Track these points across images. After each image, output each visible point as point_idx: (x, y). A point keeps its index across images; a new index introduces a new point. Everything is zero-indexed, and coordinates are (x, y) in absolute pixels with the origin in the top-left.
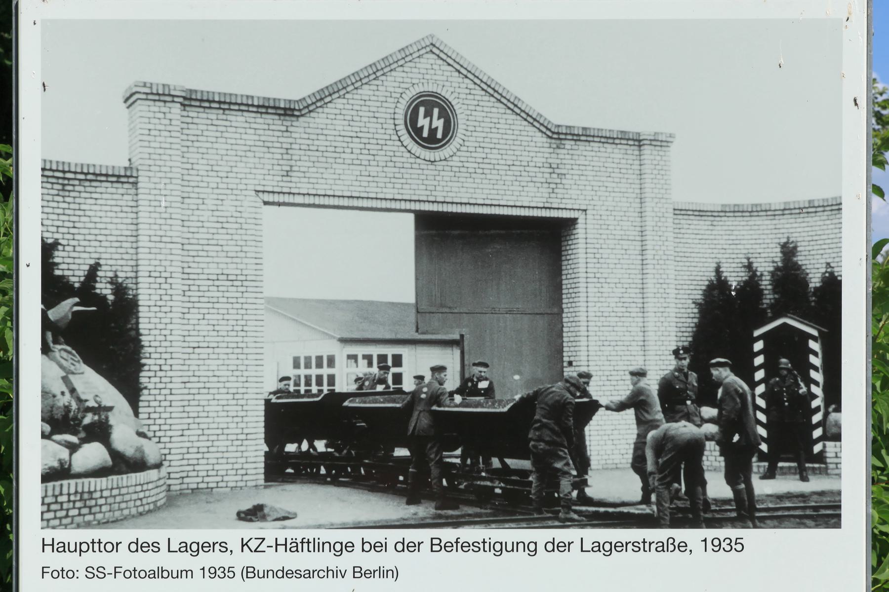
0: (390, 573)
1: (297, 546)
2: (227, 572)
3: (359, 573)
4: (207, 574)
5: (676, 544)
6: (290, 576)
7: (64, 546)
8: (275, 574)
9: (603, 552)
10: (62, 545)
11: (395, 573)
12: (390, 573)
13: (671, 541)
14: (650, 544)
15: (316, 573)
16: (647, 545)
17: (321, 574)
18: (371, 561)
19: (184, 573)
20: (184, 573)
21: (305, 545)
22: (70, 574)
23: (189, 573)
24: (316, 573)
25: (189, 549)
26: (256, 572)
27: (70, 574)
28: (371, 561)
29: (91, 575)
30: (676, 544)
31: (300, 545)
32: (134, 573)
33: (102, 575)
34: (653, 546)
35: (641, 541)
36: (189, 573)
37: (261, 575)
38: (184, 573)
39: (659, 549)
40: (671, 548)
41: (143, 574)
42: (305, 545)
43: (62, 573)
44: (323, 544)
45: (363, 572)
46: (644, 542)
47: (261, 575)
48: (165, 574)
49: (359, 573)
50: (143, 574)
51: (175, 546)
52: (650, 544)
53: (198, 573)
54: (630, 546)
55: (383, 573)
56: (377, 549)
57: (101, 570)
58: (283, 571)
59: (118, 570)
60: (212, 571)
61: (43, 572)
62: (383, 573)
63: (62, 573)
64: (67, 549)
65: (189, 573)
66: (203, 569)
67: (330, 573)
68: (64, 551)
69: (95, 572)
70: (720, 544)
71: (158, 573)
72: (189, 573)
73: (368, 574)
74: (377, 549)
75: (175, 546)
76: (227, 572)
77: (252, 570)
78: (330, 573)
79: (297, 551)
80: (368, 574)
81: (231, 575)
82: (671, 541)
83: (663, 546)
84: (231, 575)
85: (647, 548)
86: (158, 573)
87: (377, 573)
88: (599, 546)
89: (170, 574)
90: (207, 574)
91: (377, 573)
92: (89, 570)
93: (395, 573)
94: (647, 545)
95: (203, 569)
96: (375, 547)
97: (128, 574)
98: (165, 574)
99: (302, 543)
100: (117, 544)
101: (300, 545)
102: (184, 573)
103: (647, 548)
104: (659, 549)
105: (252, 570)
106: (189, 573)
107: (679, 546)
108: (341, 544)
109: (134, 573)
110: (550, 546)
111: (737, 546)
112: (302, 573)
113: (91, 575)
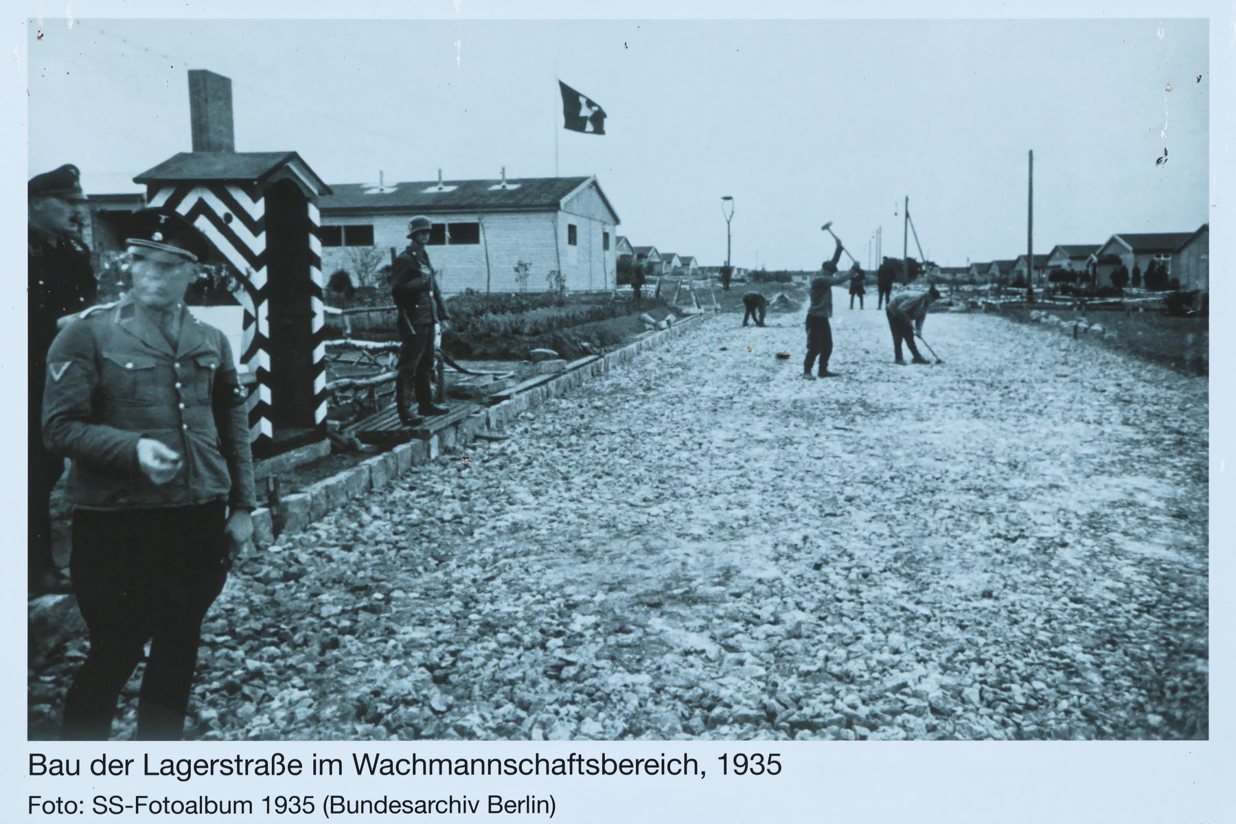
0: (543, 805)
1: (563, 766)
2: (303, 804)
3: (498, 805)
4: (273, 806)
5: (286, 763)
6: (395, 810)
7: (61, 766)
8: (373, 807)
9: (177, 775)
10: (168, 764)
11: (550, 806)
12: (543, 805)
13: (278, 759)
14: (247, 763)
15: (434, 805)
16: (242, 765)
17: (442, 807)
18: (513, 788)
19: (239, 805)
20: (239, 805)
21: (575, 764)
22: (71, 807)
23: (245, 805)
24: (434, 805)
25: (175, 771)
26: (345, 804)
27: (71, 807)
28: (513, 788)
29: (101, 809)
30: (286, 763)
31: (567, 764)
32: (165, 806)
33: (117, 809)
34: (252, 766)
35: (233, 758)
36: (245, 805)
37: (353, 808)
38: (239, 806)
39: (260, 771)
40: (278, 768)
41: (178, 807)
42: (575, 764)
44: (322, 762)
45: (503, 804)
46: (238, 760)
47: (353, 808)
48: (211, 807)
50: (178, 807)
51: (154, 766)
52: (247, 763)
53: (259, 806)
54: (217, 766)
55: (533, 805)
56: (625, 770)
57: (116, 800)
58: (385, 803)
59: (141, 801)
60: (281, 802)
61: (31, 805)
62: (533, 805)
64: (64, 771)
65: (247, 805)
66: (267, 799)
67: (455, 805)
68: (61, 773)
69: (109, 805)
70: (746, 763)
71: (200, 806)
72: (247, 806)
73: (511, 807)
74: (625, 770)
75: (154, 766)
76: (303, 804)
77: (497, 800)
78: (455, 805)
79: (563, 772)
80: (511, 807)
81: (308, 808)
82: (278, 759)
83: (266, 766)
84: (308, 808)
85: (242, 770)
86: (200, 806)
87: (524, 806)
88: (172, 766)
89: (218, 807)
90: (273, 806)
91: (524, 806)
92: (99, 800)
93: (550, 806)
94: (242, 765)
95: (267, 799)
96: (621, 766)
97: (155, 807)
98: (211, 807)
99: (571, 760)
100: (128, 763)
101: (567, 764)
102: (239, 806)
103: (242, 770)
104: (260, 771)
105: (339, 801)
106: (247, 806)
107: (290, 767)
108: (189, 762)
109: (165, 806)
110: (98, 767)
111: (770, 765)
112: (414, 806)
113: (102, 809)
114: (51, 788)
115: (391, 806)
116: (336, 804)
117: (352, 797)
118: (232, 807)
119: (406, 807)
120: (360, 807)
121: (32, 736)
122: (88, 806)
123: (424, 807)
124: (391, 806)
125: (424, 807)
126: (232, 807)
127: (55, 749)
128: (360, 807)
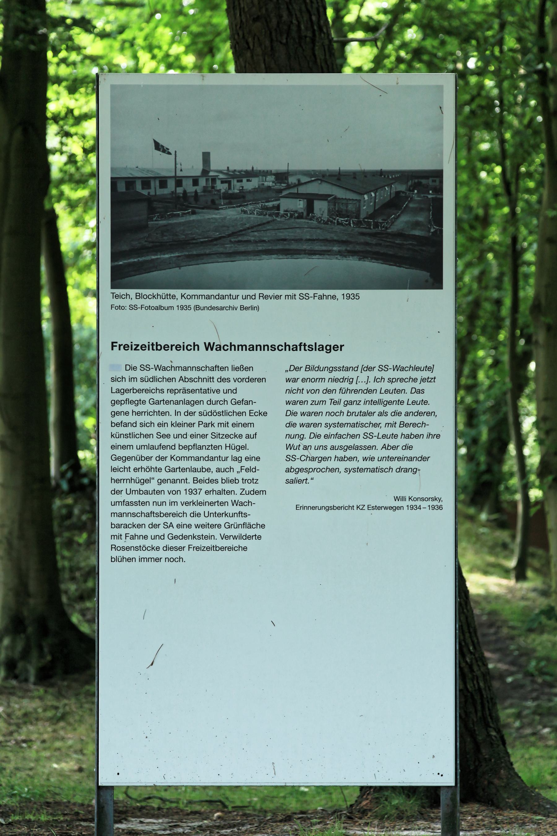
2: (188, 308)
3: (243, 308)
8: (208, 309)
11: (258, 308)
17: (227, 308)
27: (123, 308)
28: (248, 303)
32: (149, 308)
36: (172, 307)
41: (153, 308)
43: (120, 308)
49: (243, 308)
50: (153, 308)
53: (176, 308)
55: (253, 308)
62: (253, 308)
63: (120, 308)
73: (247, 308)
76: (188, 308)
80: (247, 308)
89: (164, 308)
90: (180, 308)
93: (258, 308)
98: (162, 308)
114: (118, 302)
115: (213, 308)
116: (197, 308)
117: (202, 305)
118: (168, 308)
119: (217, 308)
120: (204, 308)
121: (112, 287)
122: (128, 308)
123: (222, 308)
124: (213, 308)
125: (222, 308)
126: (168, 308)
127: (118, 291)
128: (204, 308)
